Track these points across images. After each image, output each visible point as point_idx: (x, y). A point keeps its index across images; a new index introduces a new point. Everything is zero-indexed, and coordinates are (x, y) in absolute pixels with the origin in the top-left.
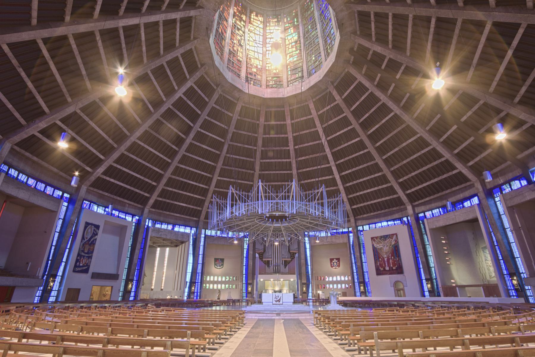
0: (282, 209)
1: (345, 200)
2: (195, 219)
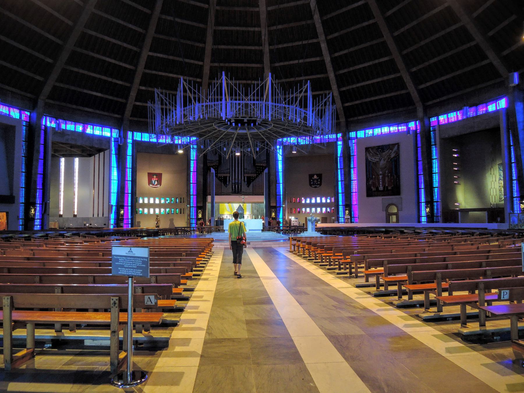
2: (116, 116)
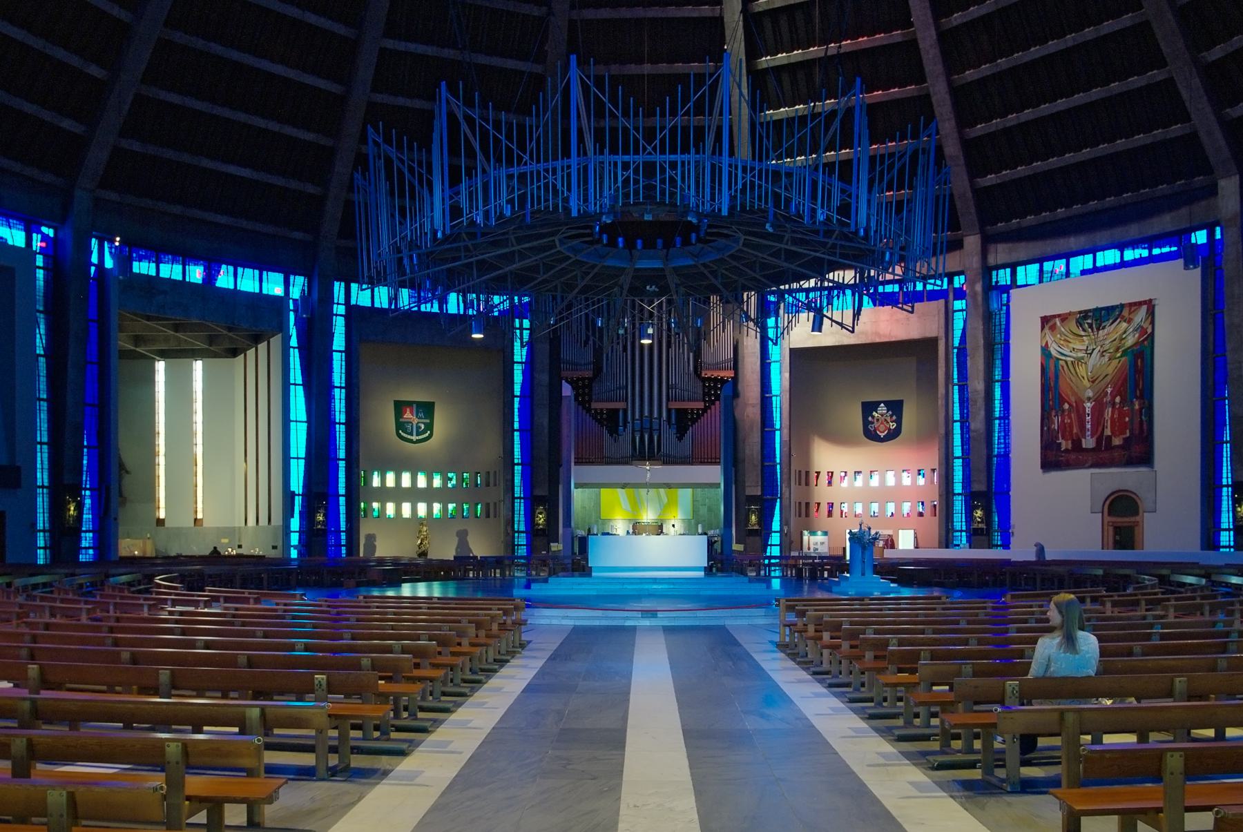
0: (672, 195)
1: (952, 148)
2: (298, 235)
